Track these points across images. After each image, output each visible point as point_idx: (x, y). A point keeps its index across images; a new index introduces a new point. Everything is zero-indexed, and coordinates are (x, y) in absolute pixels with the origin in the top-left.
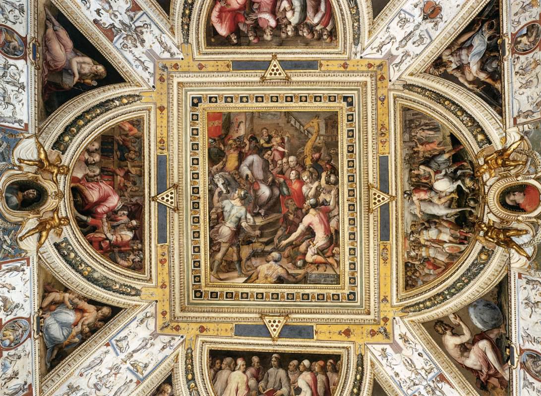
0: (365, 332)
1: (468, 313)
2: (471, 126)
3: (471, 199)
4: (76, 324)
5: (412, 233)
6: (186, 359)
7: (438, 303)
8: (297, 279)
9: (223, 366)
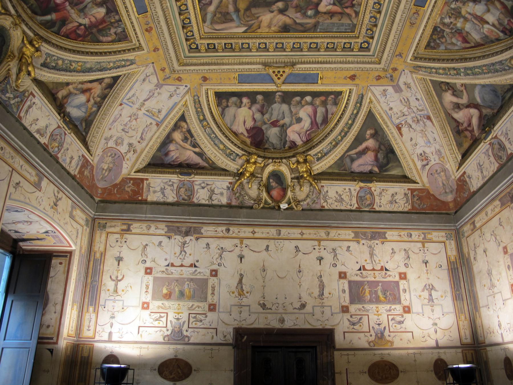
4: (88, 101)
6: (195, 104)
8: (305, 27)
9: (229, 104)
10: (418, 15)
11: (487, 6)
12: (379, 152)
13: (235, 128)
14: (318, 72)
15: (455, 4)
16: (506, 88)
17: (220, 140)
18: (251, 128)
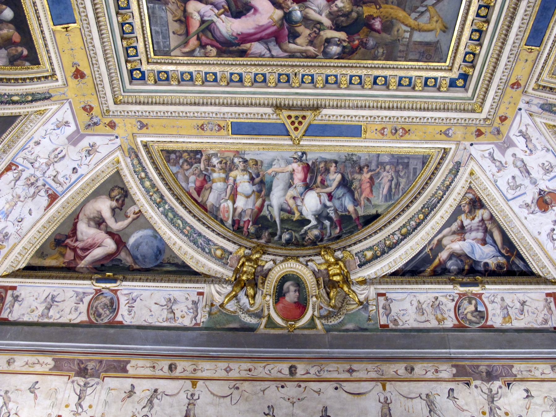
0: (86, 99)
1: (145, 229)
2: (385, 243)
3: (292, 236)
5: (245, 161)
7: (151, 196)
10: (219, 130)
11: (252, 193)
14: (78, 21)
15: (240, 162)
16: (176, 261)
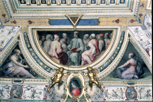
9: (47, 39)
12: (137, 66)
13: (50, 53)
17: (41, 60)
18: (60, 53)
